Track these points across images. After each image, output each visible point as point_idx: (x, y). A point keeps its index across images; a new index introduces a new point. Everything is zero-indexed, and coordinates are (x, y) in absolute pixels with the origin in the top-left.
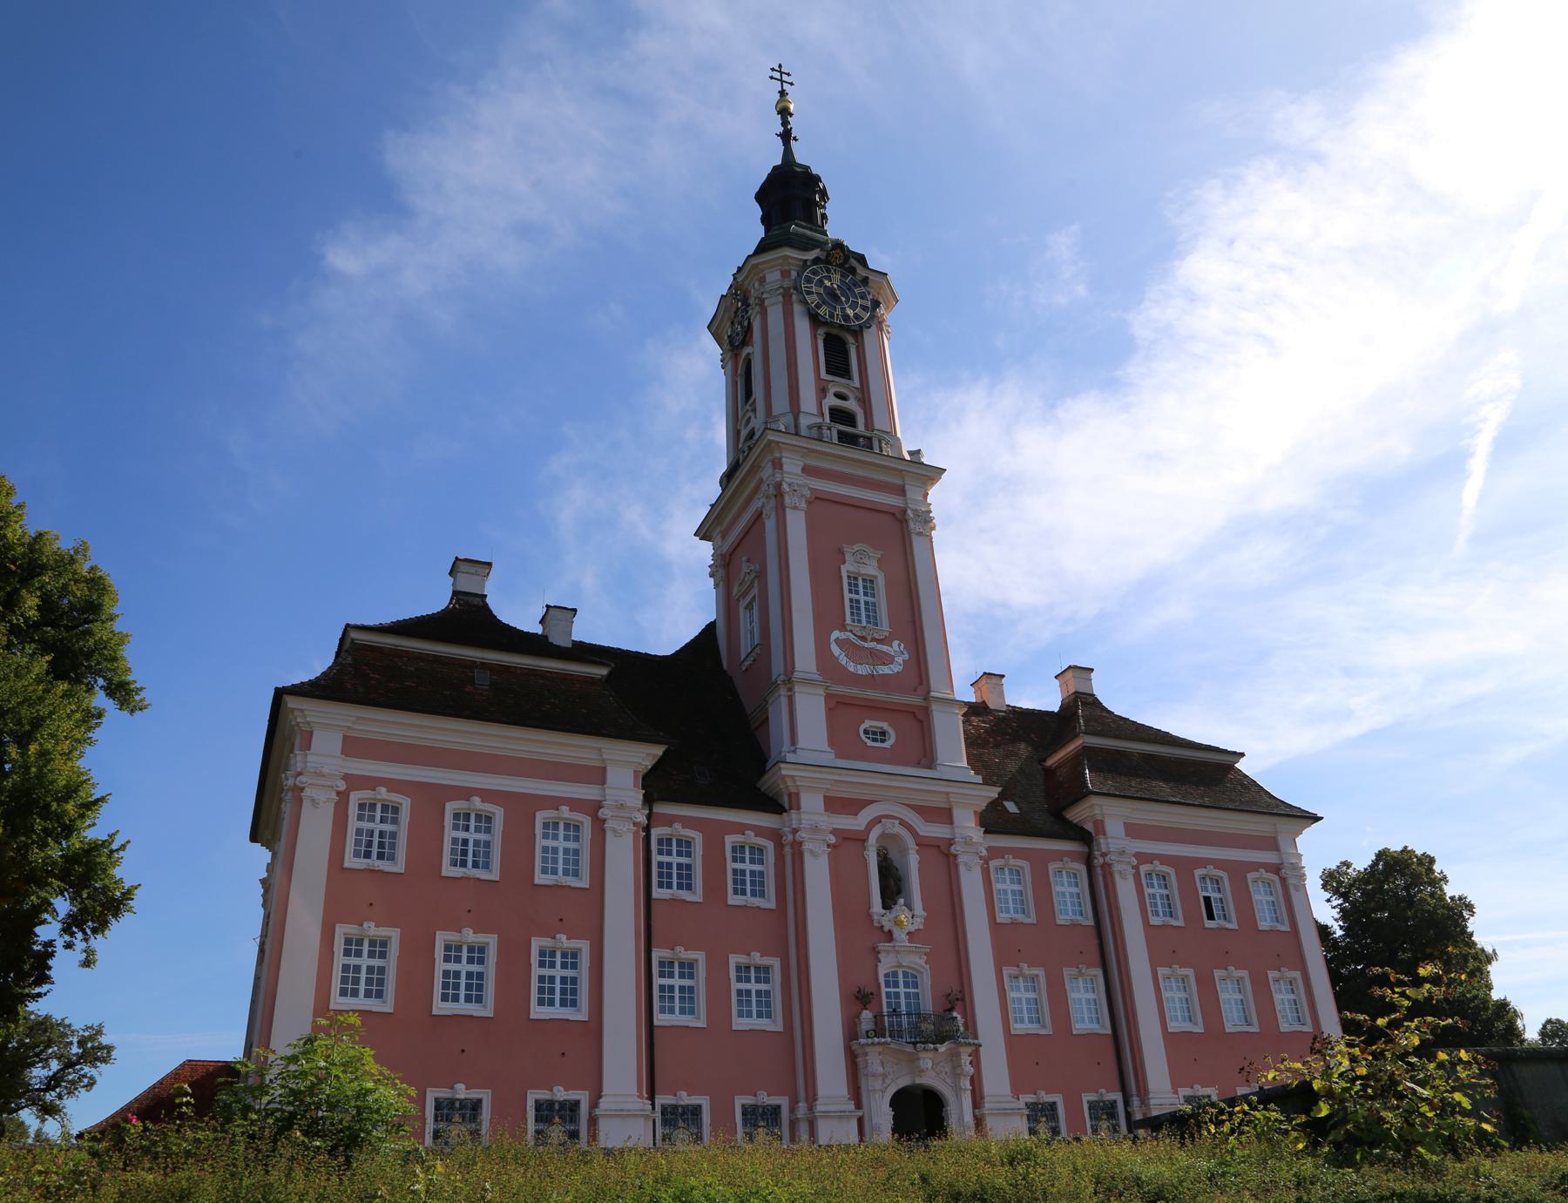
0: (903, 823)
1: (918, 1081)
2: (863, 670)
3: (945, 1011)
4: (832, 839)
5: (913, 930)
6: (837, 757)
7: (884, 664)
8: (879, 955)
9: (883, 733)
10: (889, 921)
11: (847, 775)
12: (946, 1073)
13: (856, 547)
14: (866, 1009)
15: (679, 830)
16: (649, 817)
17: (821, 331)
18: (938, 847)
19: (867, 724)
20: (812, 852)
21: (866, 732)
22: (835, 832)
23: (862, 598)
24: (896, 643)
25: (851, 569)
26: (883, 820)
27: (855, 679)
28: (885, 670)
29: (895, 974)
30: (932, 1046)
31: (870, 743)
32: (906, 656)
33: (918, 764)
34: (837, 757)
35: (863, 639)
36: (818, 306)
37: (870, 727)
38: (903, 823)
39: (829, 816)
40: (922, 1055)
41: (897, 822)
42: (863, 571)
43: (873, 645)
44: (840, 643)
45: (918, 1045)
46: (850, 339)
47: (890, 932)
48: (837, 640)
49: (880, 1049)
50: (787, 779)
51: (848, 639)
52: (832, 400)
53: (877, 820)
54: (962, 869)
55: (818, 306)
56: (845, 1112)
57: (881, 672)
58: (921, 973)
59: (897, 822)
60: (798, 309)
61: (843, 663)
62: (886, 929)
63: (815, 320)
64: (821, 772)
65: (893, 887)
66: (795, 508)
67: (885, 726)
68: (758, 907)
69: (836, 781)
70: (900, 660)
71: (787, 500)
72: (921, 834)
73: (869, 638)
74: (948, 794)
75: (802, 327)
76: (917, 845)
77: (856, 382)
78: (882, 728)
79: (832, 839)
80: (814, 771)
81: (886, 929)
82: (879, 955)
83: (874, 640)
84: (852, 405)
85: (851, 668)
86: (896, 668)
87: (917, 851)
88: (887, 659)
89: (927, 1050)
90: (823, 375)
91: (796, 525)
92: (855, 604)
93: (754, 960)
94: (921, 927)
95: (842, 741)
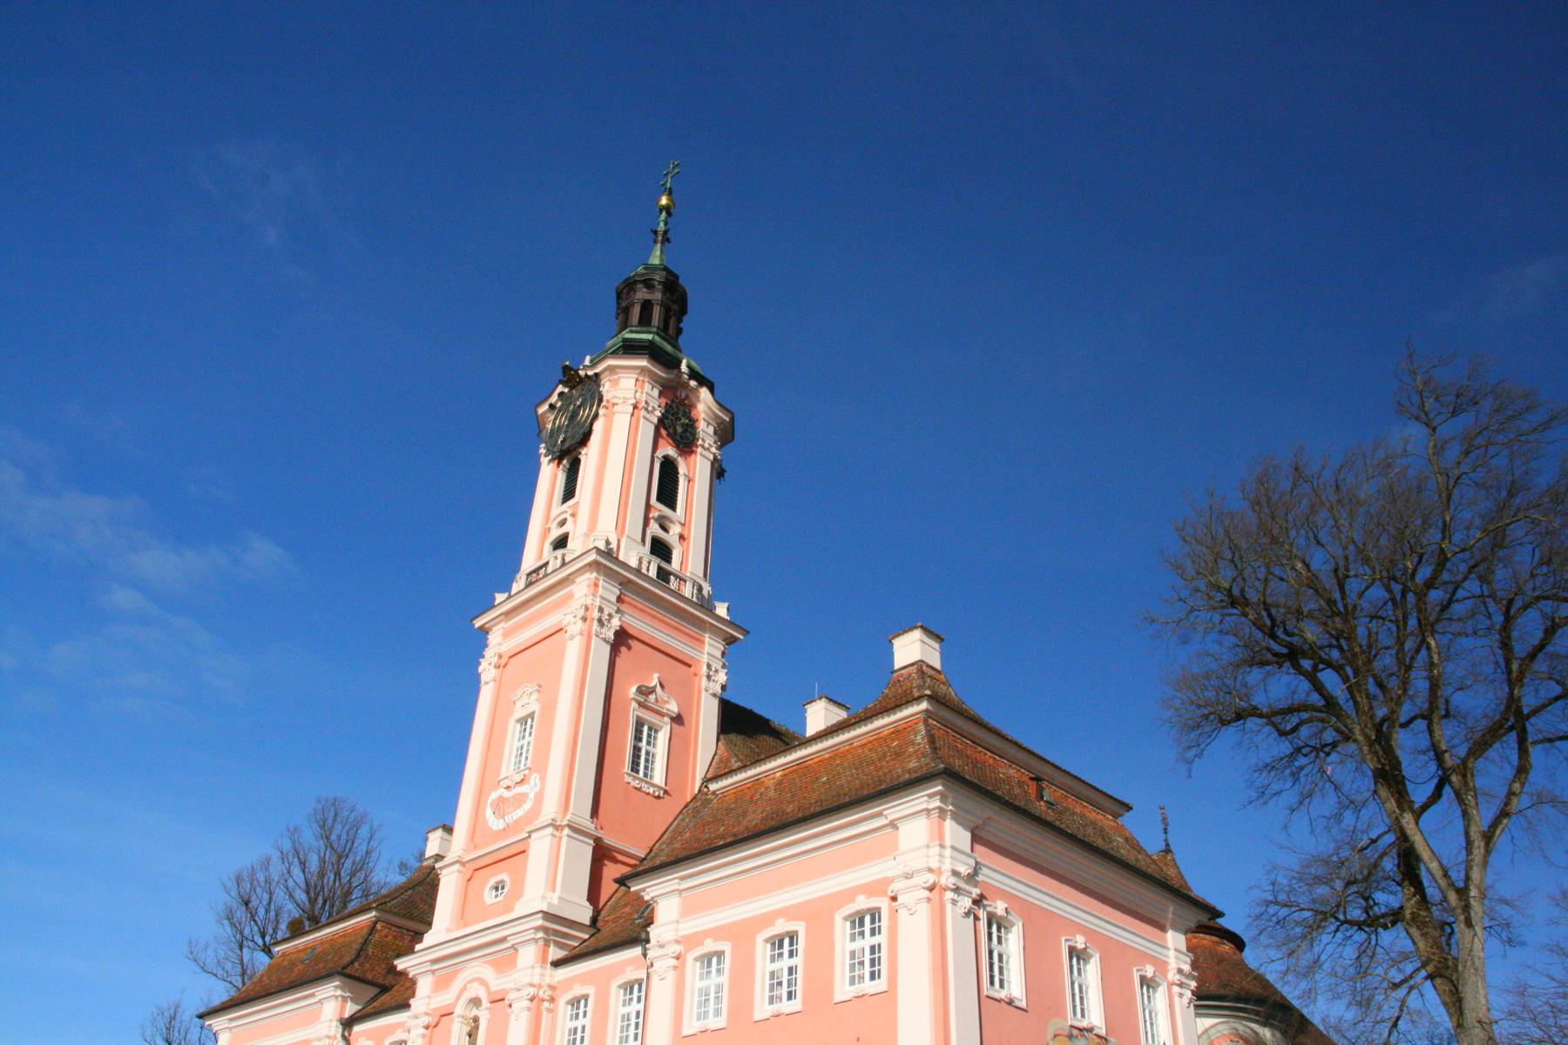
7: (519, 807)
13: (519, 693)
19: (492, 882)
28: (519, 813)
35: (508, 788)
37: (497, 883)
38: (483, 982)
52: (556, 533)
53: (464, 989)
57: (515, 817)
59: (476, 984)
61: (490, 824)
70: (532, 796)
79: (426, 1020)
88: (520, 800)
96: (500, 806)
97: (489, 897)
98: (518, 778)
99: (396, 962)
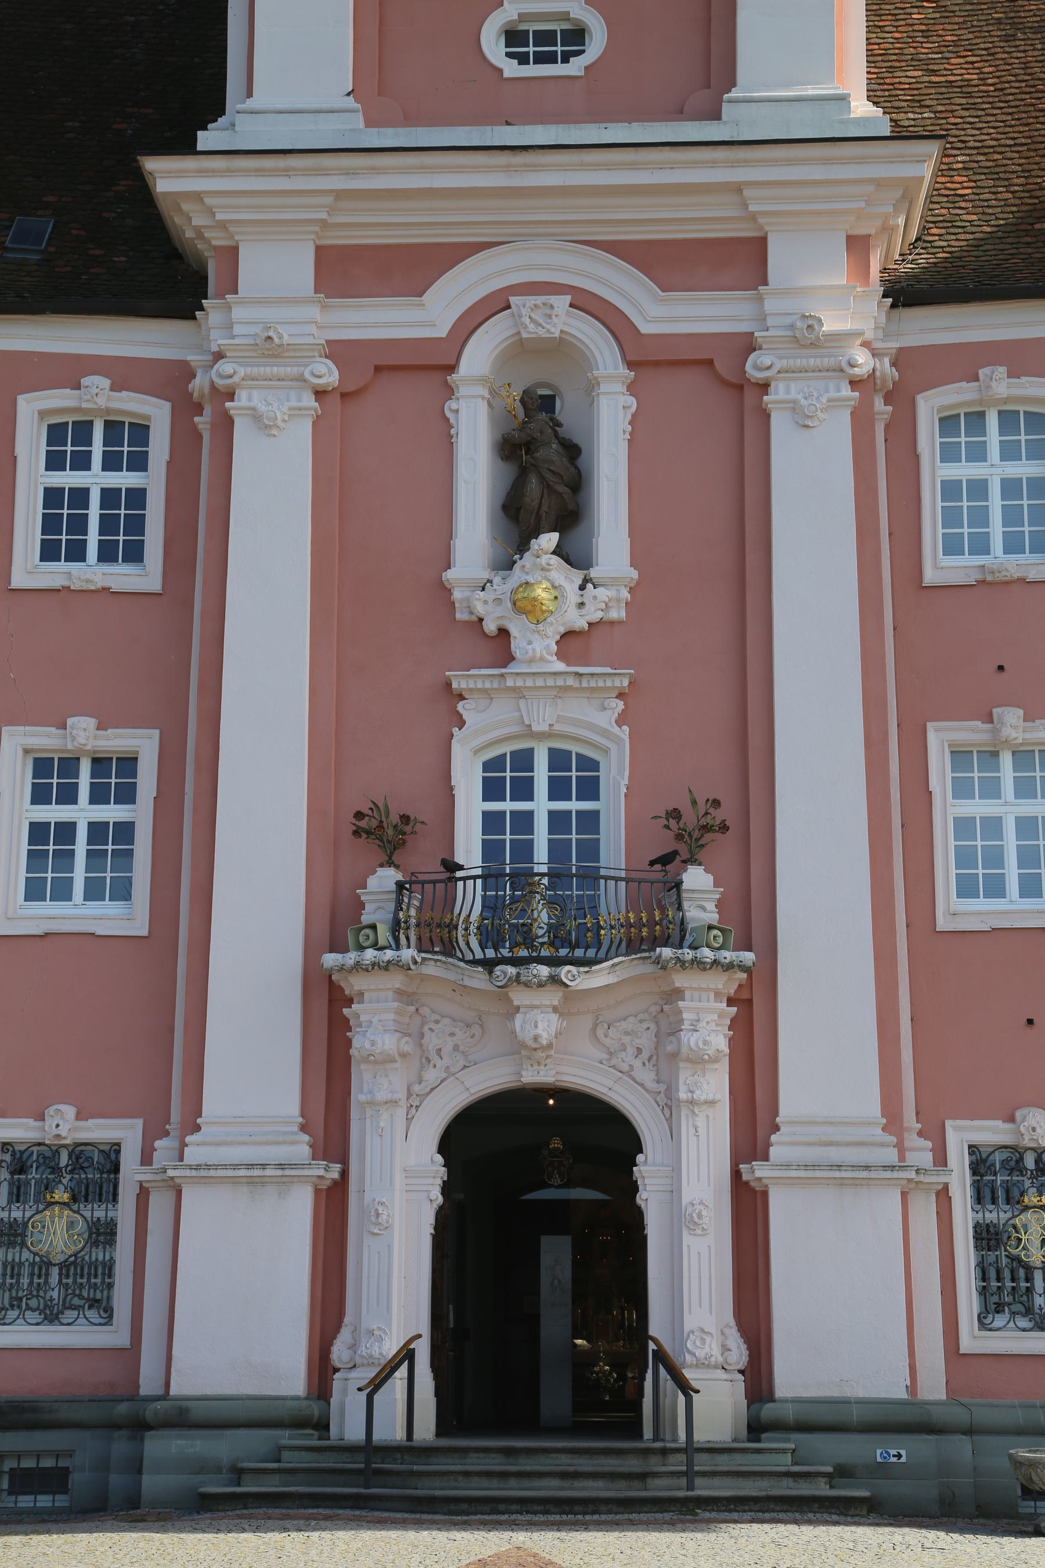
1: (533, 1076)
3: (652, 863)
4: (328, 374)
5: (581, 624)
6: (369, 123)
8: (460, 706)
9: (577, 36)
10: (498, 601)
11: (375, 170)
12: (639, 1051)
14: (390, 863)
18: (710, 363)
20: (256, 416)
21: (513, 37)
26: (514, 300)
29: (524, 760)
30: (544, 971)
31: (511, 69)
33: (679, 113)
34: (369, 123)
37: (523, 17)
39: (324, 307)
40: (519, 997)
45: (498, 970)
47: (503, 633)
49: (396, 980)
50: (185, 207)
54: (780, 425)
56: (264, 1166)
58: (606, 751)
62: (490, 627)
64: (286, 172)
68: (105, 589)
69: (340, 195)
72: (645, 328)
74: (738, 188)
76: (630, 365)
78: (565, 17)
79: (328, 374)
80: (260, 172)
81: (490, 627)
82: (460, 706)
87: (632, 388)
89: (527, 985)
93: (74, 739)
94: (618, 613)
97: (494, 48)
99: (151, 164)
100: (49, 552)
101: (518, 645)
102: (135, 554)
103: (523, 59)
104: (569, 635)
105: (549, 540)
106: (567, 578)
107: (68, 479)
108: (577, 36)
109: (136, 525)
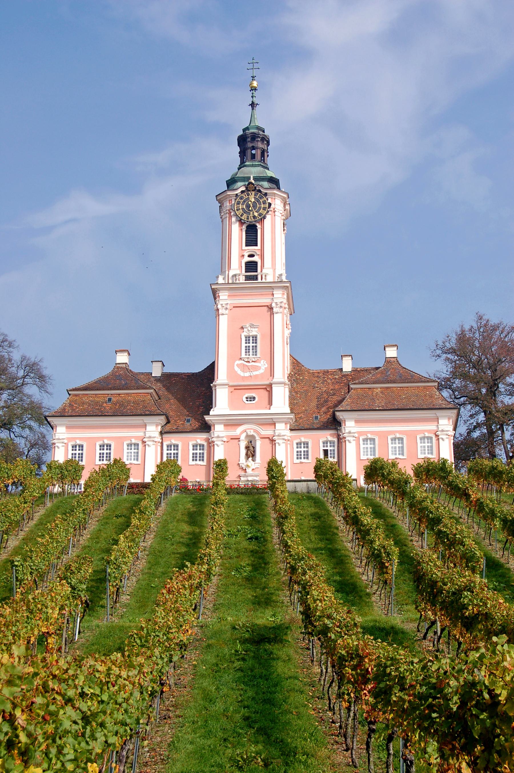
0: (255, 431)
2: (247, 374)
7: (257, 371)
9: (254, 398)
15: (174, 442)
16: (162, 439)
17: (244, 227)
19: (246, 395)
20: (217, 445)
21: (247, 398)
22: (227, 436)
23: (251, 345)
24: (262, 361)
25: (246, 334)
27: (244, 378)
32: (266, 366)
35: (249, 362)
36: (241, 216)
38: (255, 431)
41: (252, 431)
42: (251, 334)
43: (253, 364)
44: (237, 365)
46: (259, 226)
48: (237, 365)
51: (242, 364)
52: (247, 259)
55: (241, 216)
60: (234, 219)
63: (241, 222)
65: (251, 452)
66: (223, 314)
67: (254, 395)
71: (220, 311)
73: (251, 361)
75: (236, 228)
77: (259, 247)
79: (225, 439)
83: (253, 361)
84: (256, 259)
85: (242, 374)
86: (261, 371)
88: (257, 368)
90: (244, 247)
91: (223, 321)
92: (247, 349)
95: (232, 404)
96: (243, 368)
97: (245, 400)
98: (254, 360)
99: (205, 416)
100: (193, 460)
101: (247, 470)
102: (203, 460)
103: (248, 401)
104: (253, 469)
105: (250, 459)
106: (253, 463)
107: (195, 451)
108: (254, 398)
109: (203, 457)
